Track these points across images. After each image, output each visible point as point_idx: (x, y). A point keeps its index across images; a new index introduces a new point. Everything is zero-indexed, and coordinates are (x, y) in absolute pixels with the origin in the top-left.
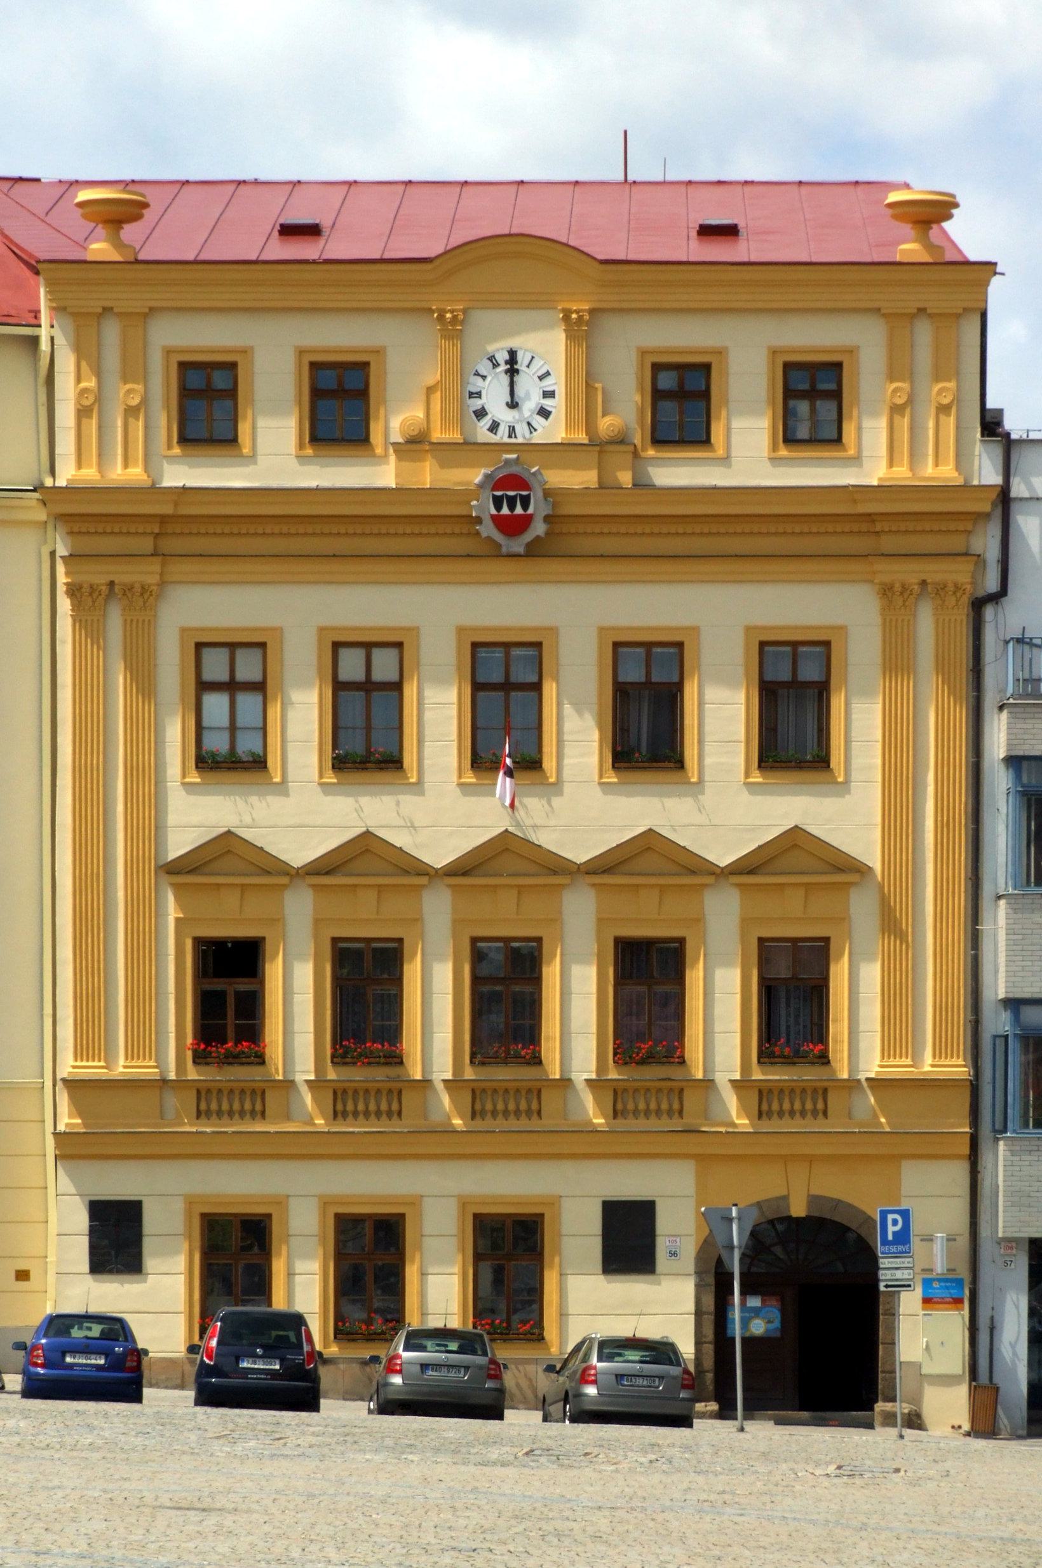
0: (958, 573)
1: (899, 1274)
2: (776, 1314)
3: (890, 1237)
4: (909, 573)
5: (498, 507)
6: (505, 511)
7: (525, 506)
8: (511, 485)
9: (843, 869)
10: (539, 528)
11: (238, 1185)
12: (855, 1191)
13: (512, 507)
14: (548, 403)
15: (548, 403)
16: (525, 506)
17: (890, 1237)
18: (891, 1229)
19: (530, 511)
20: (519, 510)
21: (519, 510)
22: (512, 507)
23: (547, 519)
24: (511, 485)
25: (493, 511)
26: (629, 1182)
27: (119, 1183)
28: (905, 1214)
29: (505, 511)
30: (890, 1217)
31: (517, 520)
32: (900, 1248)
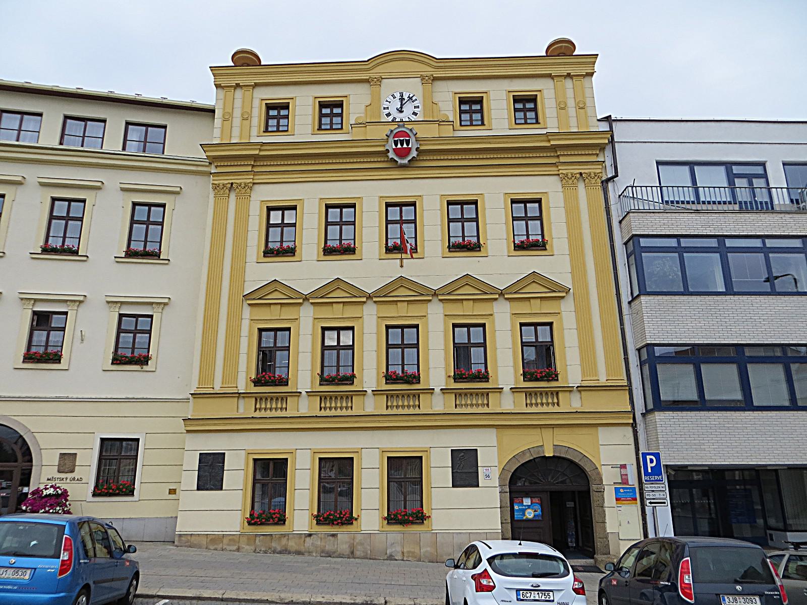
0: (597, 169)
1: (657, 495)
2: (538, 507)
3: (650, 471)
4: (576, 170)
5: (396, 145)
6: (399, 146)
7: (408, 144)
8: (401, 136)
9: (556, 292)
10: (414, 153)
11: (271, 445)
12: (576, 443)
13: (402, 145)
14: (416, 110)
15: (416, 110)
16: (408, 144)
17: (650, 471)
18: (649, 465)
19: (410, 146)
20: (405, 146)
21: (405, 146)
22: (402, 145)
23: (417, 149)
24: (401, 136)
25: (394, 147)
26: (464, 440)
27: (212, 444)
28: (657, 455)
29: (399, 146)
30: (648, 457)
31: (403, 153)
32: (656, 477)
